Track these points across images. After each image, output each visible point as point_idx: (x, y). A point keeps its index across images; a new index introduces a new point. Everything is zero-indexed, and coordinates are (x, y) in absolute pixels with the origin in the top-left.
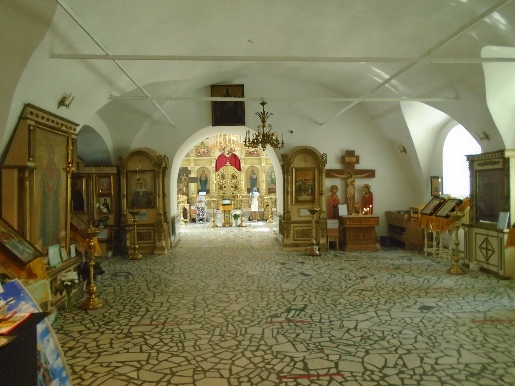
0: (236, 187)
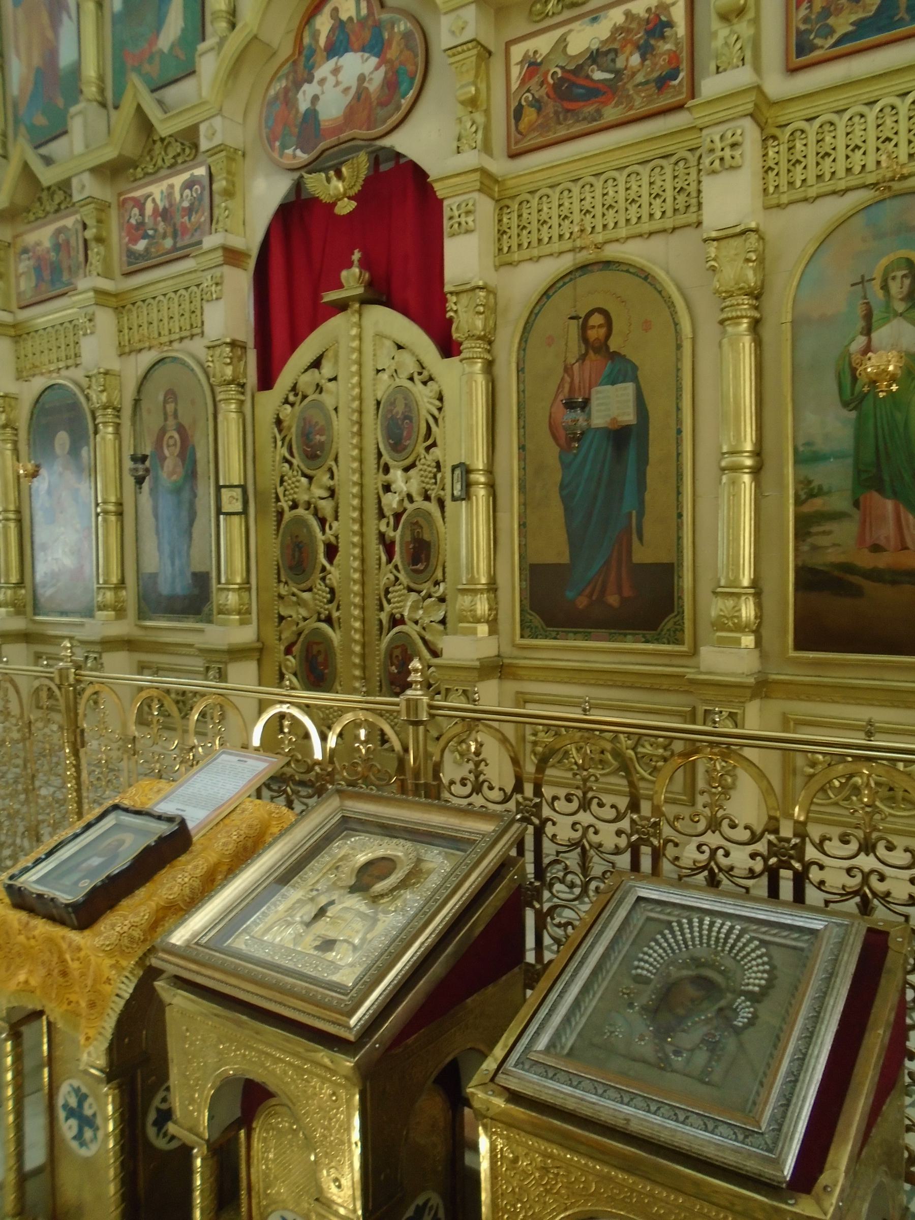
0: (422, 553)
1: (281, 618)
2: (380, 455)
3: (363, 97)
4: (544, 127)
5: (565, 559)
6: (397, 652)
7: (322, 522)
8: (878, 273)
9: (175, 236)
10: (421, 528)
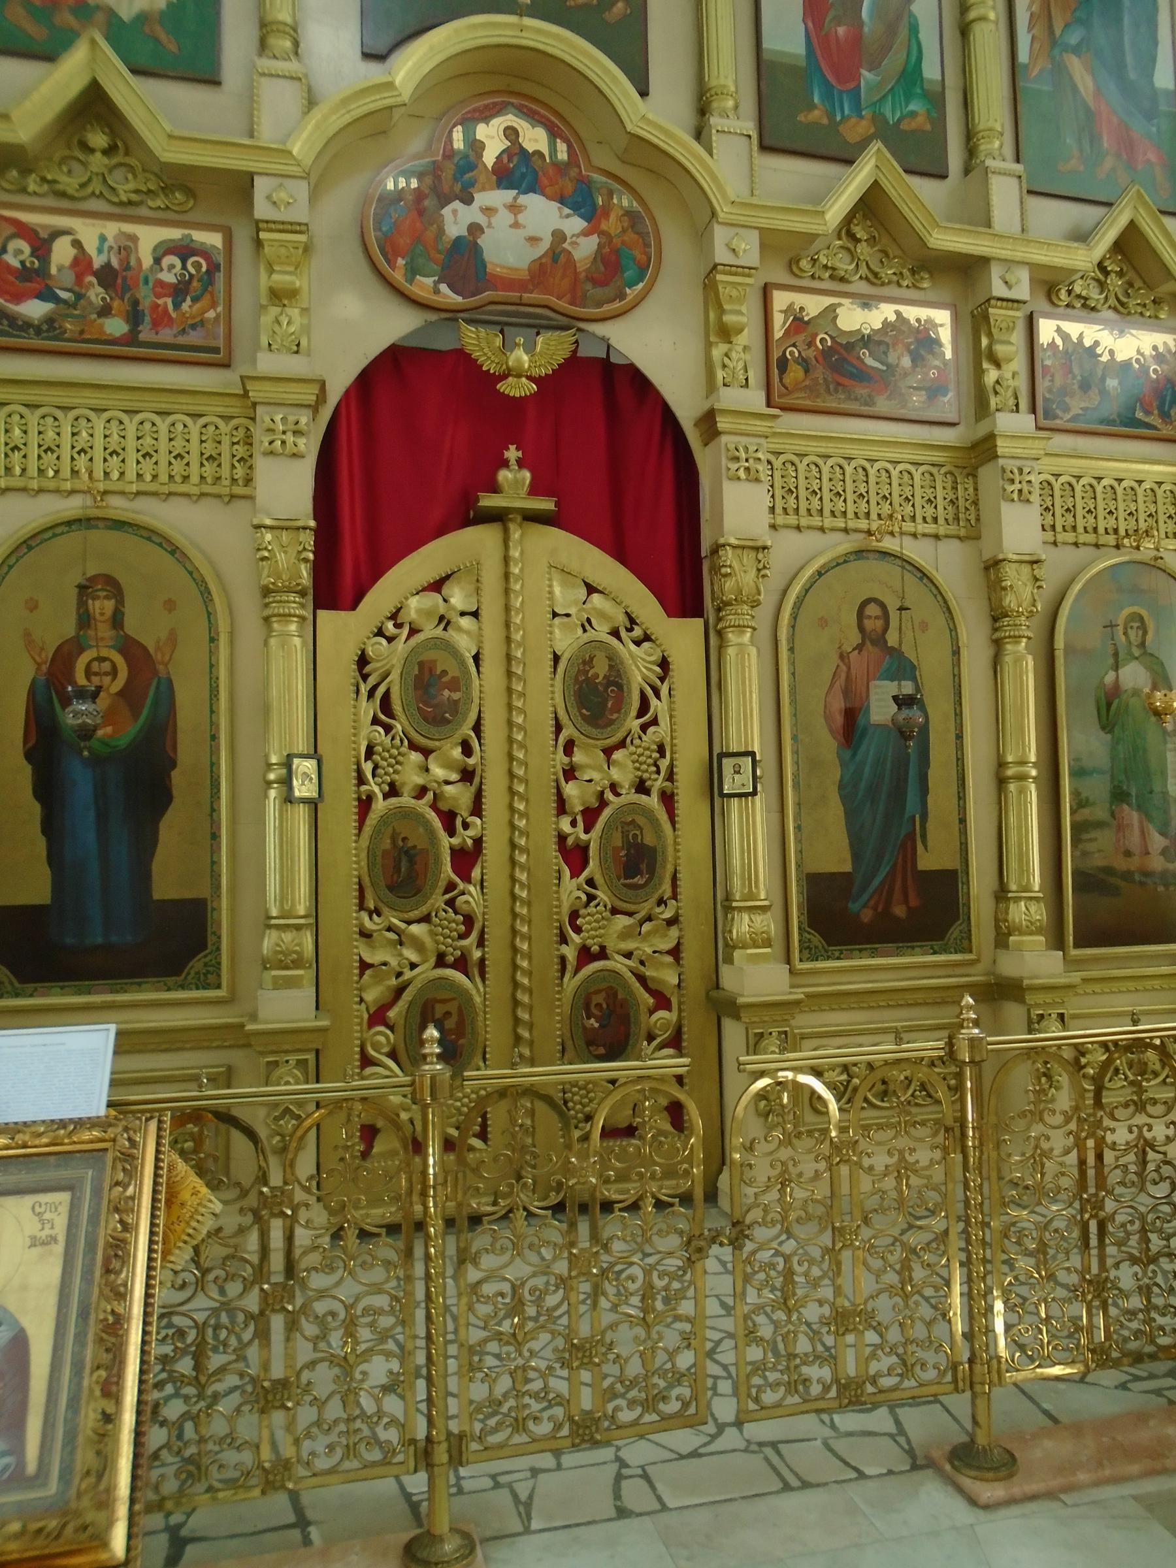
0: (638, 862)
1: (364, 966)
2: (558, 728)
3: (562, 259)
4: (812, 390)
5: (847, 867)
6: (599, 999)
7: (449, 819)
8: (1121, 621)
9: (134, 317)
10: (641, 829)
